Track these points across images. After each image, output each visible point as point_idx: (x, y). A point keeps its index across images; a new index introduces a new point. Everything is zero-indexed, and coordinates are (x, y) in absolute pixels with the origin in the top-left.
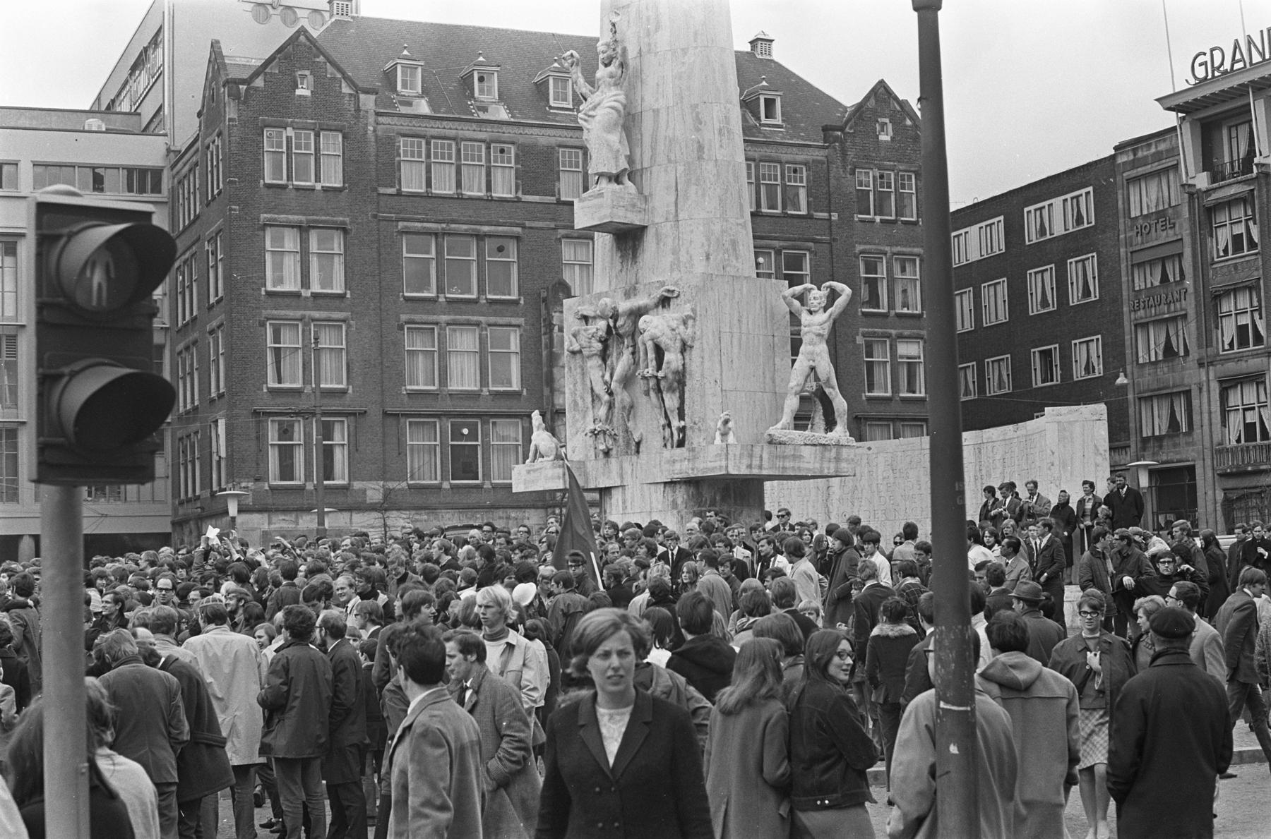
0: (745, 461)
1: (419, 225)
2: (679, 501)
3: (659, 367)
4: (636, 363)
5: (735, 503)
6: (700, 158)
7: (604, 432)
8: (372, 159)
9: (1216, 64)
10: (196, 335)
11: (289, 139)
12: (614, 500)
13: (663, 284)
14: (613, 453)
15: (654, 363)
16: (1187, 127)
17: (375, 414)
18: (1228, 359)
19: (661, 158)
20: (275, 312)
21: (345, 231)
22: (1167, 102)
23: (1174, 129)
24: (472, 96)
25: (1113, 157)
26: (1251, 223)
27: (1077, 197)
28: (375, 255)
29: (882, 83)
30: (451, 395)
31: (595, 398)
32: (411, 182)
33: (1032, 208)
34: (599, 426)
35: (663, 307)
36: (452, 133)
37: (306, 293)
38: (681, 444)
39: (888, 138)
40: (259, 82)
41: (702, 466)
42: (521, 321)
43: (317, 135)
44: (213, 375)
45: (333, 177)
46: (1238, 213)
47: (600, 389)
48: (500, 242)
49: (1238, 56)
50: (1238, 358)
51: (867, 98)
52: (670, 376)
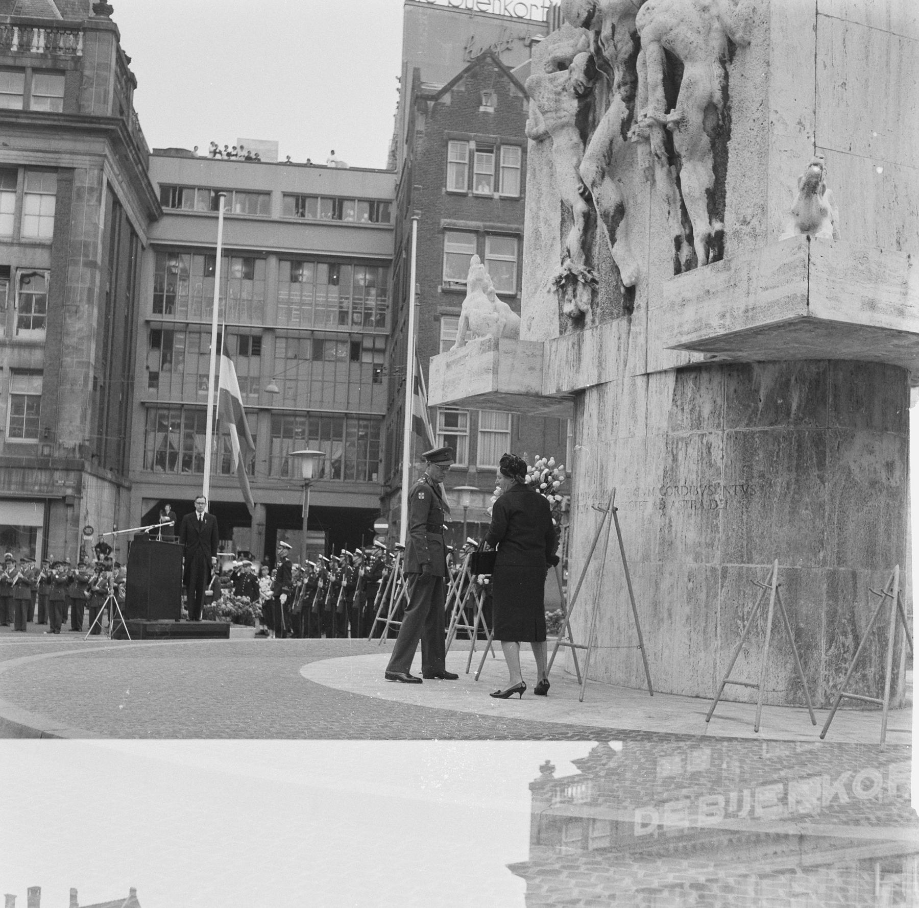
2: (706, 410)
3: (671, 102)
14: (588, 318)
15: (660, 93)
20: (449, 309)
40: (447, 99)
52: (695, 118)
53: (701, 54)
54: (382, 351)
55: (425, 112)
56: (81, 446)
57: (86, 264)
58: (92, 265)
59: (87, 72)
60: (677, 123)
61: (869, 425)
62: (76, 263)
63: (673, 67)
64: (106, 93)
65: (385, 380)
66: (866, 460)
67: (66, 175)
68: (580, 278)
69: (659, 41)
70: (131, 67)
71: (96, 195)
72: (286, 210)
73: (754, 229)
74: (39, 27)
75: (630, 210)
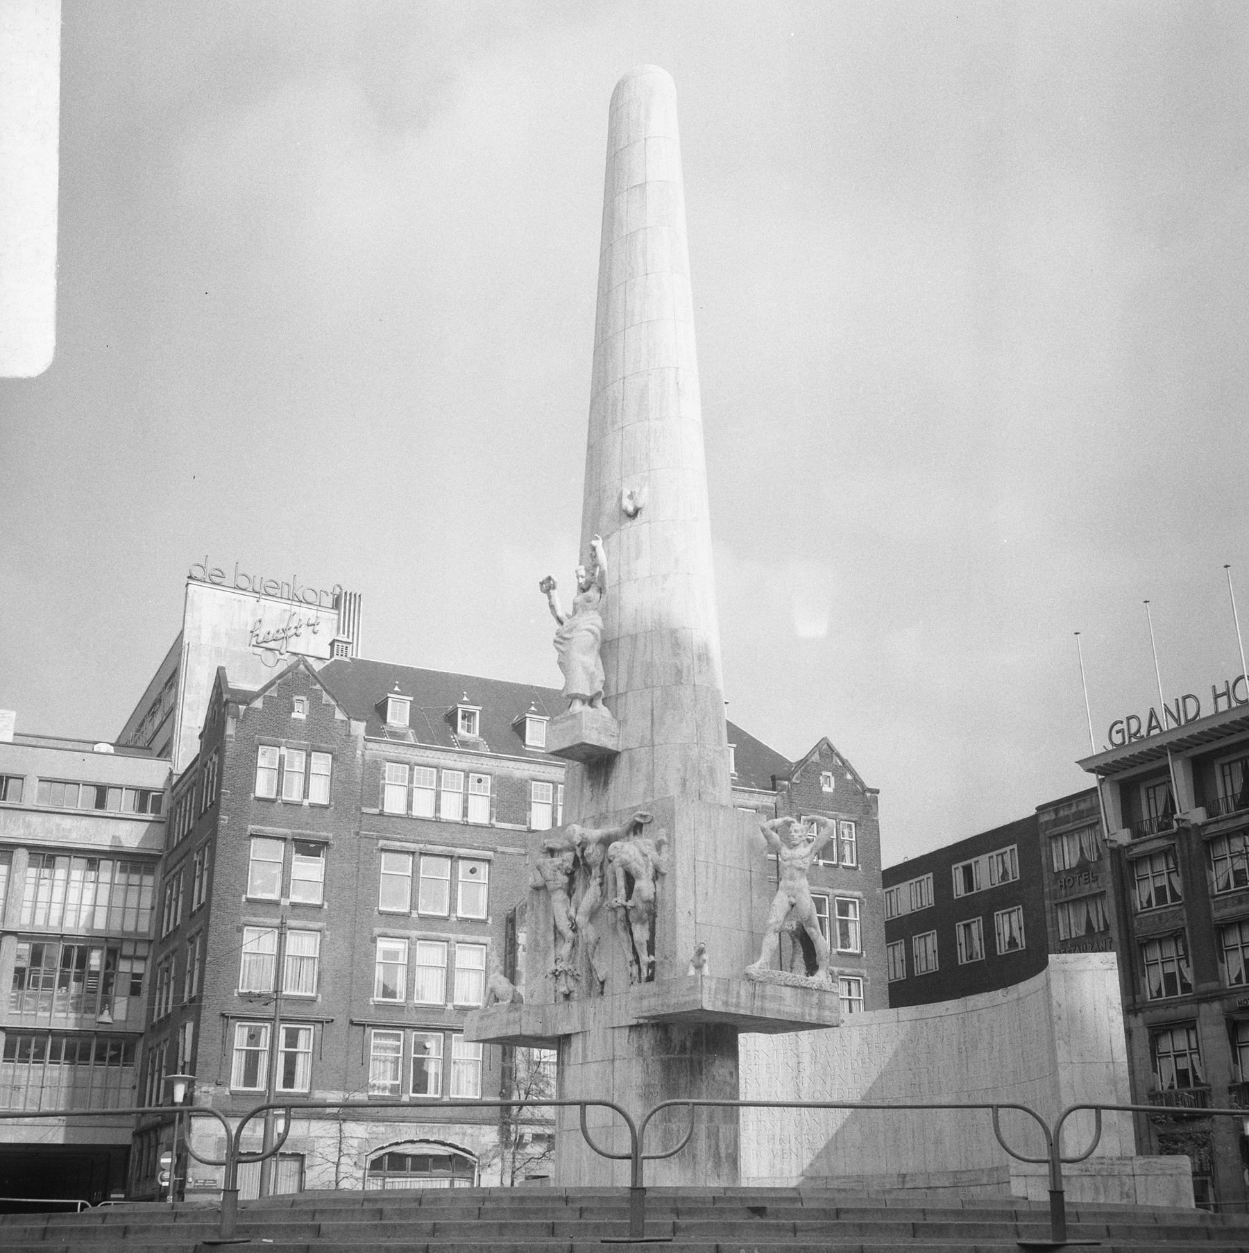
0: (722, 997)
1: (398, 844)
4: (604, 895)
5: (709, 1052)
6: (679, 682)
7: (566, 973)
8: (359, 780)
9: (1133, 731)
10: (177, 944)
11: (281, 758)
13: (634, 809)
14: (575, 995)
16: (1107, 787)
17: (341, 1021)
18: (1156, 1006)
19: (638, 682)
22: (1089, 765)
23: (1095, 789)
24: (455, 731)
25: (1035, 817)
26: (1173, 876)
27: (1002, 854)
28: (354, 870)
29: (824, 740)
30: (419, 1009)
33: (960, 865)
34: (561, 966)
35: (635, 834)
36: (435, 761)
37: (285, 902)
38: (650, 979)
39: (830, 790)
40: (258, 704)
41: (673, 1001)
42: (488, 940)
44: (188, 982)
45: (320, 793)
46: (1161, 865)
47: (564, 925)
49: (1154, 723)
50: (1167, 1005)
51: (812, 753)
52: (641, 906)
54: (145, 959)
65: (145, 995)
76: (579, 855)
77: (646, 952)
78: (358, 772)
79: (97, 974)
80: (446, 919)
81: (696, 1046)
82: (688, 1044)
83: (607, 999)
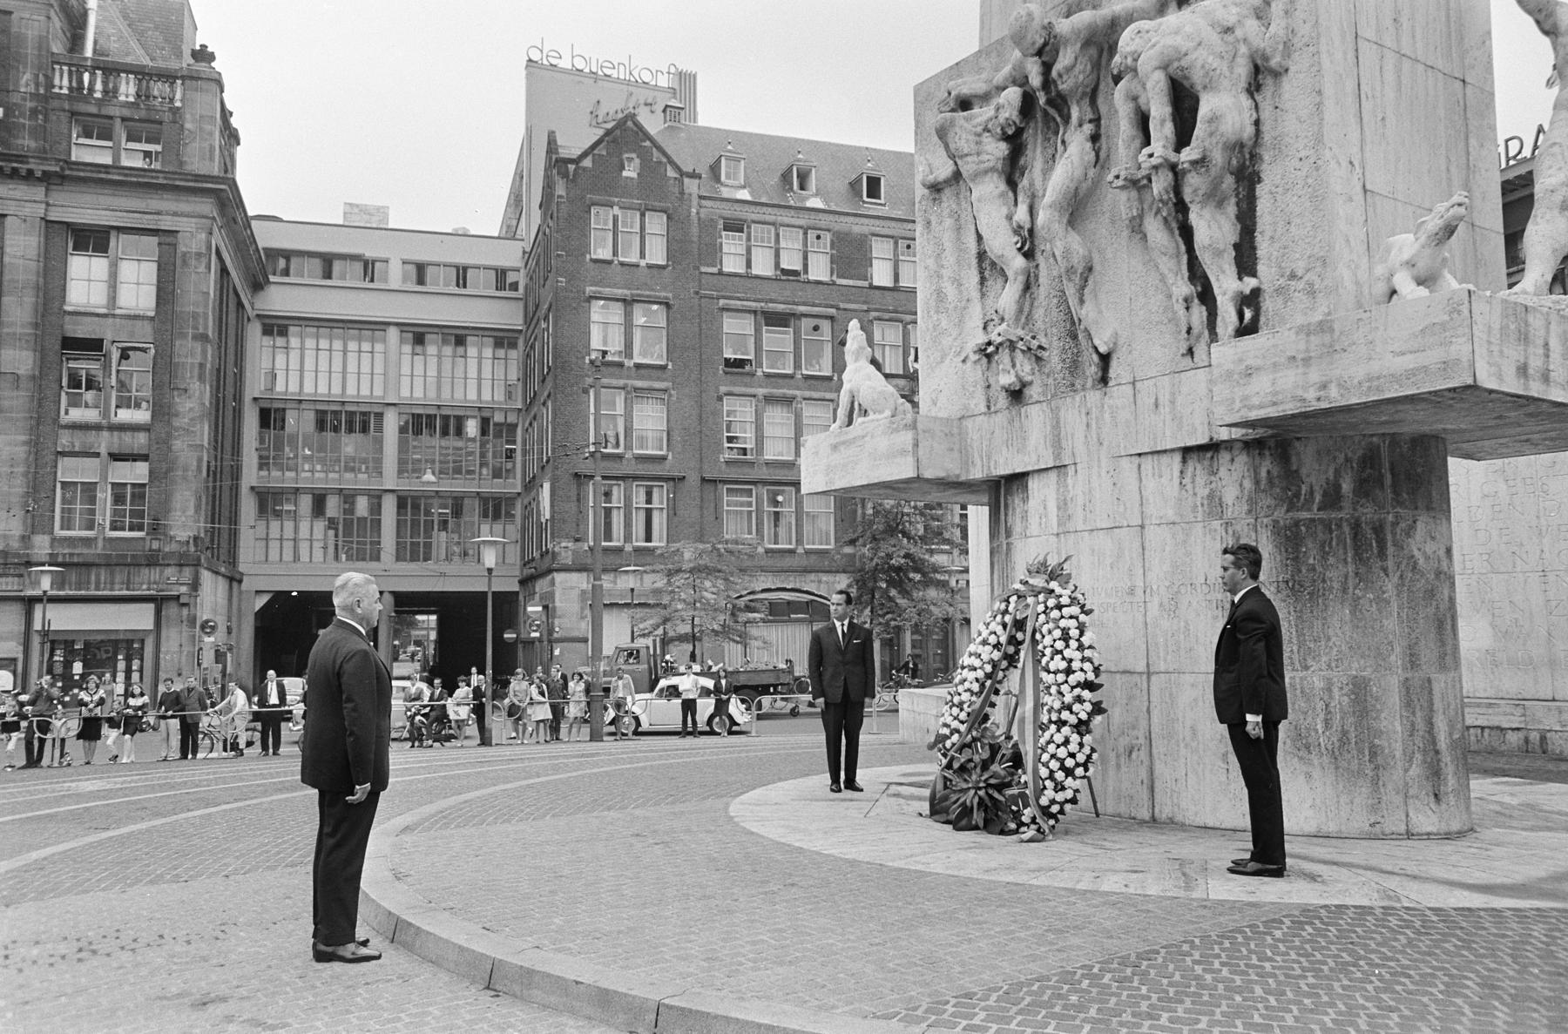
0: (1514, 354)
2: (1230, 494)
3: (1183, 138)
4: (1100, 160)
5: (1398, 502)
7: (1012, 346)
11: (615, 219)
12: (1034, 503)
14: (1033, 392)
15: (1169, 128)
17: (693, 479)
21: (668, 305)
31: (988, 267)
32: (732, 265)
40: (587, 163)
41: (1359, 372)
43: (643, 215)
45: (657, 254)
48: (813, 322)
52: (1218, 157)
53: (1226, 83)
55: (565, 175)
56: (196, 538)
57: (195, 338)
58: (203, 338)
59: (188, 126)
60: (1194, 163)
61: (1429, 508)
62: (183, 336)
63: (1184, 101)
64: (212, 148)
66: (1430, 548)
67: (169, 240)
68: (1020, 345)
69: (1165, 67)
70: (234, 122)
71: (204, 261)
72: (405, 279)
73: (1311, 285)
74: (128, 72)
75: (1097, 267)
76: (1036, 81)
77: (1231, 270)
78: (695, 230)
79: (473, 440)
80: (791, 377)
81: (1364, 488)
82: (1346, 486)
83: (1119, 393)
